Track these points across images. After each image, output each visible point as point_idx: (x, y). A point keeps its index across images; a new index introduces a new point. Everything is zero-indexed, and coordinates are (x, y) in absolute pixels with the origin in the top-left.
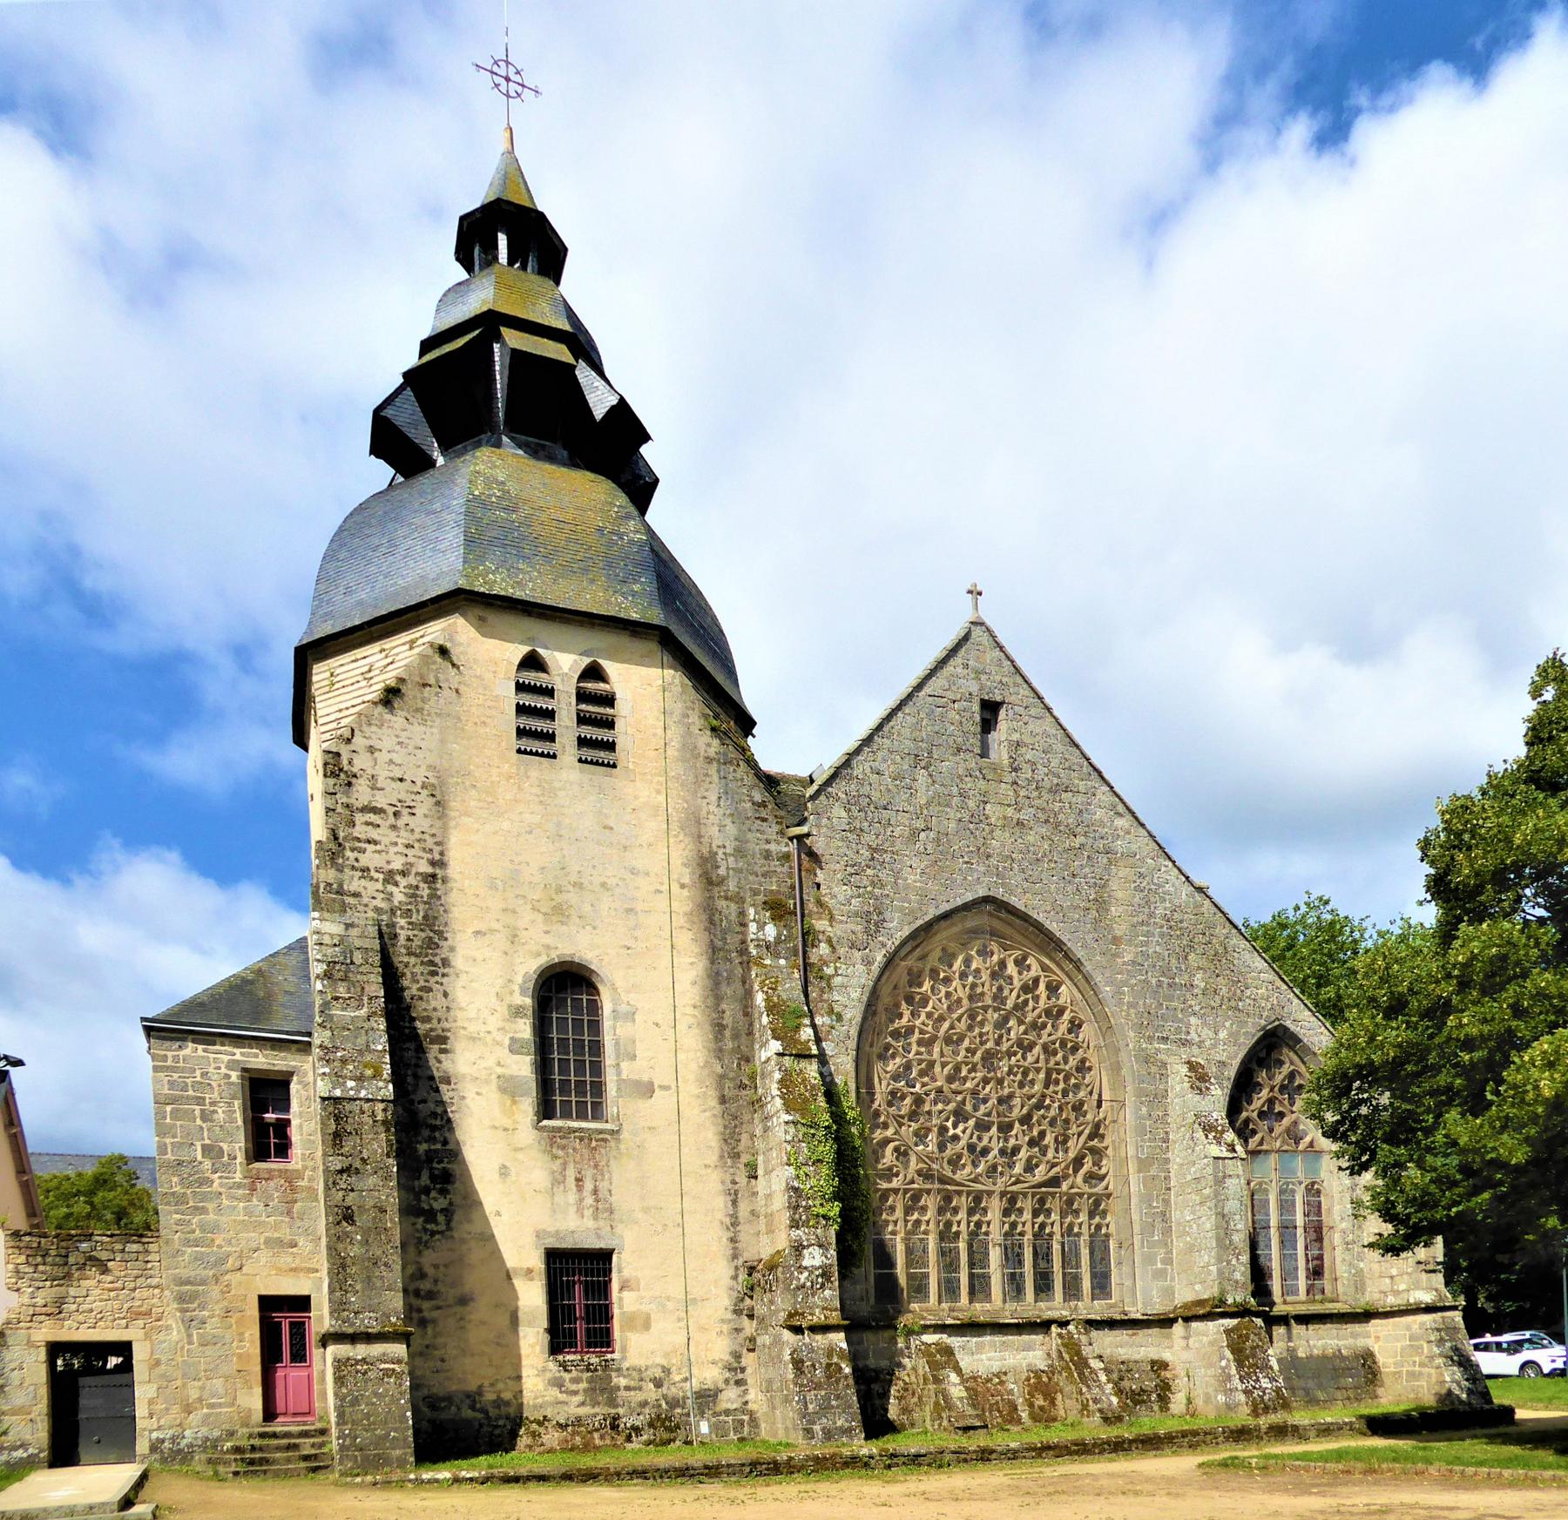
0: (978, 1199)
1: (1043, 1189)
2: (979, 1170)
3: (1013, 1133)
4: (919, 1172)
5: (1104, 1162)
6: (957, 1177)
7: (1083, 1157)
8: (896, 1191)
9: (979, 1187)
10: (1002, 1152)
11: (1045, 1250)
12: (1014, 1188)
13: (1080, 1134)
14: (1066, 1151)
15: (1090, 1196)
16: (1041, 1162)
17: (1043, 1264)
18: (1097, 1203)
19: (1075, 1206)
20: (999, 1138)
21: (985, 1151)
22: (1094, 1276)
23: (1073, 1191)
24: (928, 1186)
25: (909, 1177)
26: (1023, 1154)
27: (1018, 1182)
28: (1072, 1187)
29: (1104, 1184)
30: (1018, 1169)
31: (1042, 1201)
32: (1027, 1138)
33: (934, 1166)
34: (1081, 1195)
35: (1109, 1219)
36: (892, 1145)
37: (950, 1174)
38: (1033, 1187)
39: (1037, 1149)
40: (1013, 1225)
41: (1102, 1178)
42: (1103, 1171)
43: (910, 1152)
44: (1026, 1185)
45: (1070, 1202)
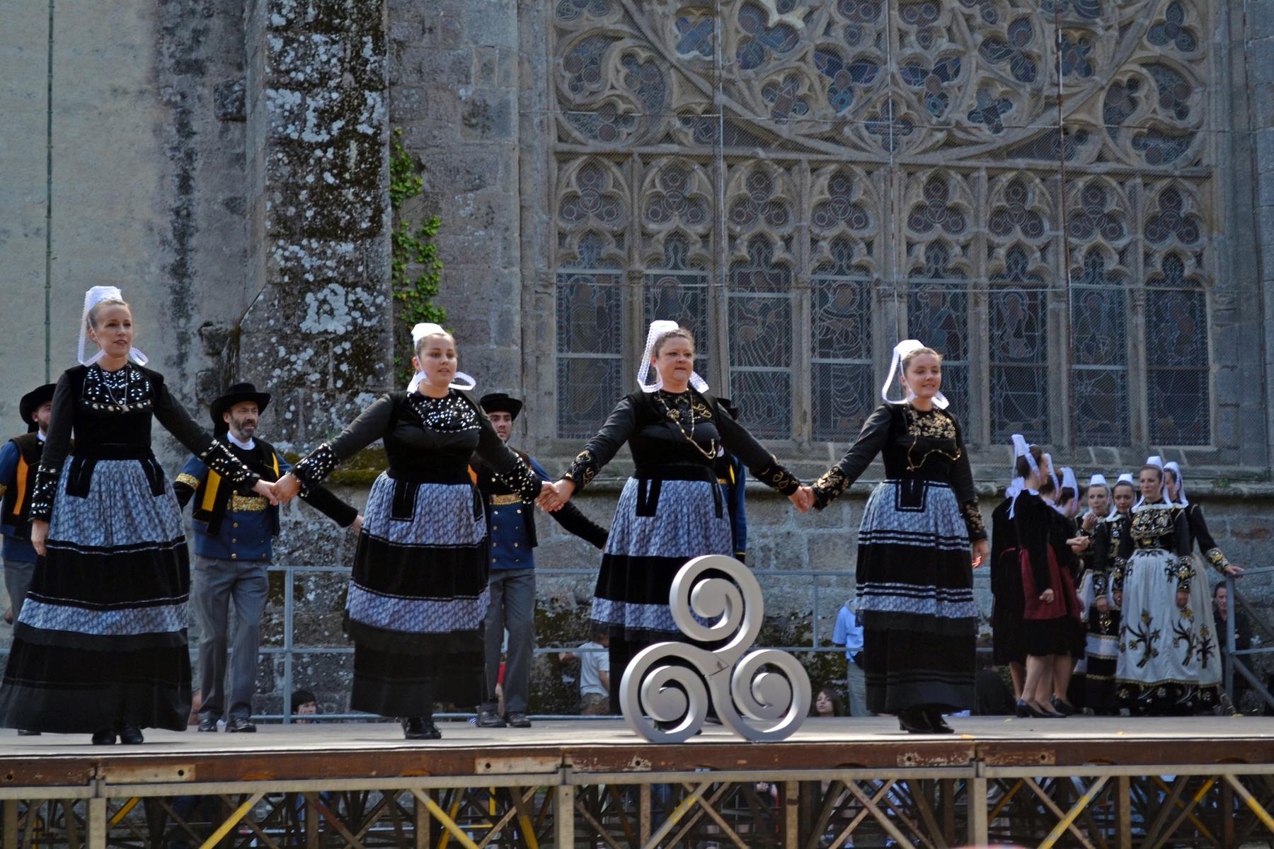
0: (842, 180)
1: (1021, 162)
2: (846, 112)
3: (942, 21)
4: (686, 116)
5: (1194, 101)
6: (784, 130)
7: (1134, 84)
8: (620, 159)
9: (845, 153)
10: (914, 69)
11: (1022, 313)
12: (939, 158)
13: (1124, 28)
14: (1088, 70)
15: (1149, 179)
16: (1017, 94)
17: (1018, 350)
18: (1171, 196)
19: (1111, 206)
20: (903, 36)
21: (863, 68)
22: (1159, 378)
23: (1102, 167)
24: (706, 150)
25: (661, 129)
26: (974, 70)
27: (950, 143)
28: (1100, 158)
29: (1189, 152)
30: (956, 113)
31: (1017, 188)
32: (979, 38)
33: (721, 99)
34: (1123, 177)
35: (1203, 239)
36: (617, 49)
37: (763, 118)
38: (993, 154)
39: (1004, 68)
40: (938, 247)
41: (1186, 137)
42: (1192, 119)
43: (664, 67)
44: (973, 150)
45: (1096, 191)
